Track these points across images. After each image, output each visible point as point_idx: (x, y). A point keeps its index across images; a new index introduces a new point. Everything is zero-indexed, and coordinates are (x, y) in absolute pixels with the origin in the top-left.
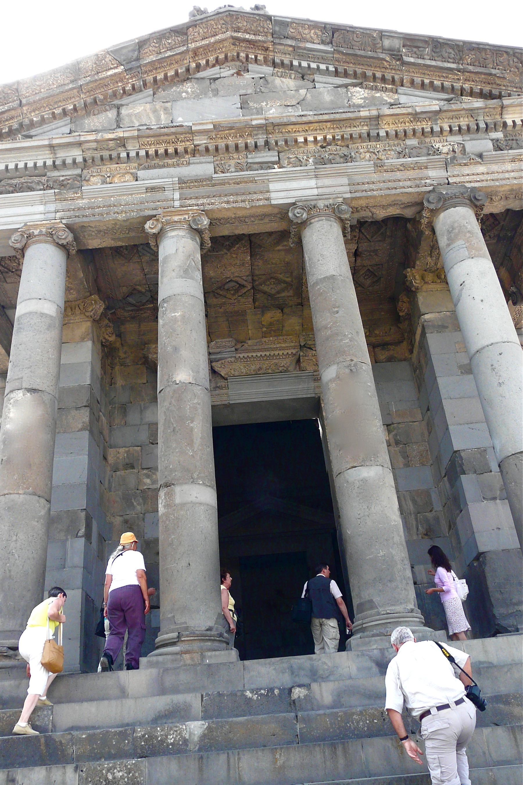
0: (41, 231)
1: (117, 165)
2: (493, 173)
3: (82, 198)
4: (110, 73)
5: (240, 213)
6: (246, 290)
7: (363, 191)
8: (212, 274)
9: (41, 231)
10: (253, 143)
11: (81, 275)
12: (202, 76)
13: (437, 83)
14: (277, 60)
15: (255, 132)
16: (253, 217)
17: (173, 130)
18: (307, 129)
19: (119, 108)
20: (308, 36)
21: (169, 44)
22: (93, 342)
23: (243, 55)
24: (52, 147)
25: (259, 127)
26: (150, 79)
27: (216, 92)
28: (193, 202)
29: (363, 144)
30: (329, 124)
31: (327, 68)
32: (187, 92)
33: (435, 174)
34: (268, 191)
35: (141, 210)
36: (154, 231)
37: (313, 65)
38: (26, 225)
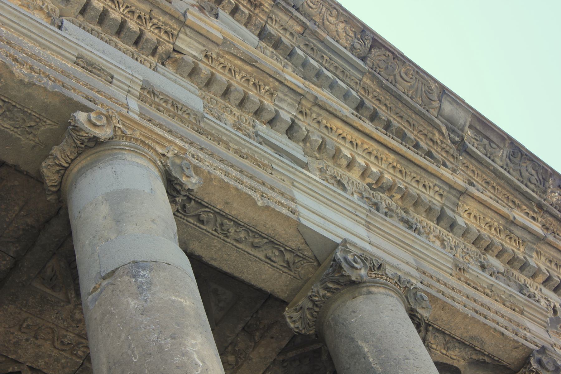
5: (237, 210)
16: (248, 230)
18: (359, 143)
20: (332, 27)
30: (392, 157)
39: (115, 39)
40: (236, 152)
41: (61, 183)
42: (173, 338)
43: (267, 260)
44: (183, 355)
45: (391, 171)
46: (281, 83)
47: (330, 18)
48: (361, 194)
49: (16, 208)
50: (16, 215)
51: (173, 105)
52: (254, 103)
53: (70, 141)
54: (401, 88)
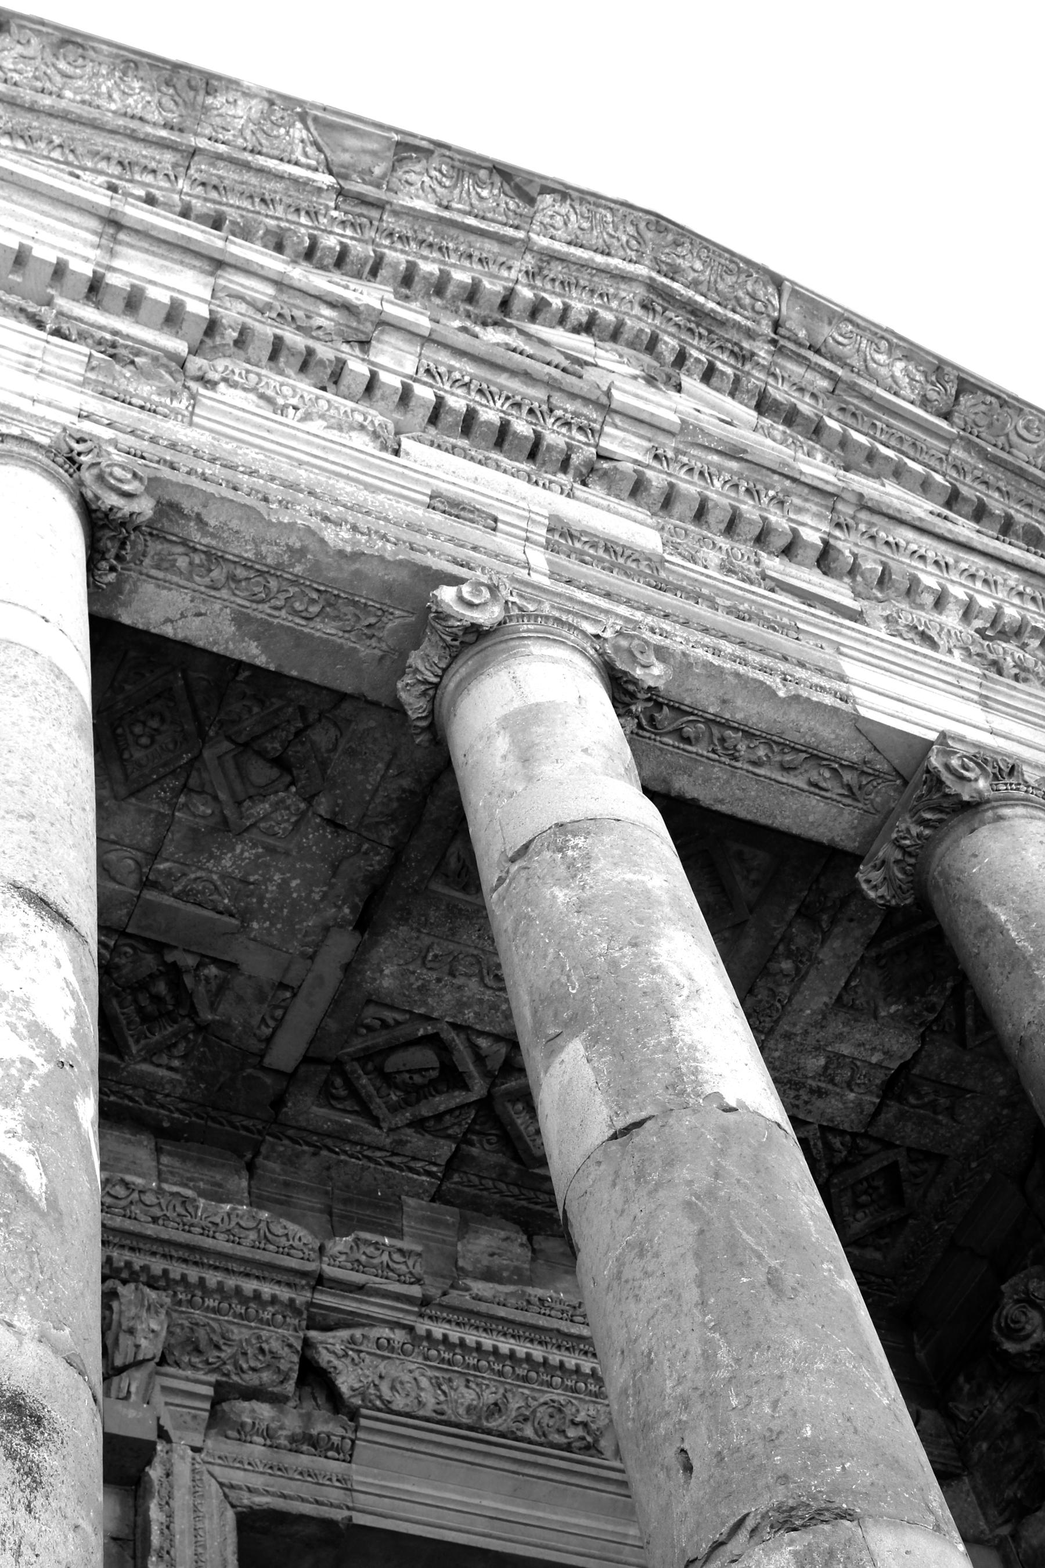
6: (459, 1097)
8: (387, 976)
15: (797, 501)
16: (769, 743)
20: (883, 371)
21: (481, 198)
23: (669, 344)
24: (113, 224)
26: (397, 257)
37: (883, 450)
39: (494, 455)
40: (729, 611)
41: (432, 712)
42: (635, 945)
43: (812, 789)
44: (654, 971)
45: (1016, 601)
46: (794, 480)
47: (877, 356)
48: (967, 649)
49: (380, 765)
50: (383, 777)
51: (606, 550)
52: (751, 522)
53: (435, 638)
54: (1020, 457)
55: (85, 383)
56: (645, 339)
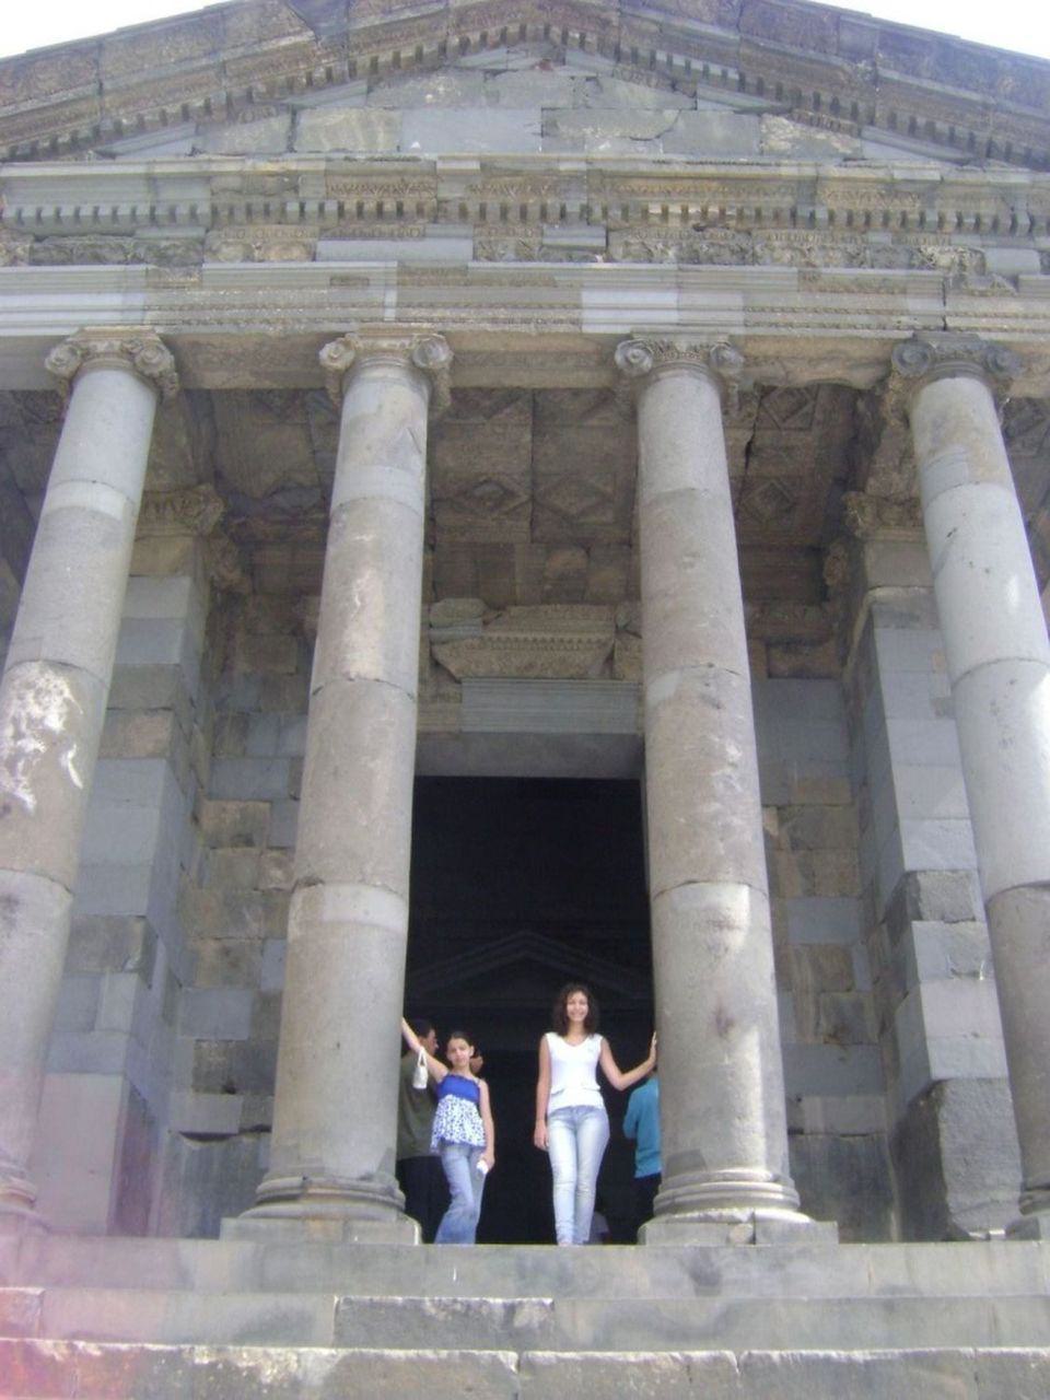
0: (111, 345)
1: (278, 226)
2: (1036, 317)
3: (200, 285)
4: (285, 42)
5: (517, 345)
7: (771, 325)
8: (450, 462)
9: (111, 345)
10: (558, 206)
11: (183, 440)
12: (469, 64)
13: (941, 126)
14: (625, 48)
17: (398, 166)
18: (670, 189)
19: (294, 113)
22: (195, 580)
23: (556, 31)
24: (151, 180)
25: (574, 177)
26: (363, 60)
27: (494, 99)
28: (424, 313)
29: (778, 232)
30: (715, 184)
31: (725, 74)
32: (435, 92)
33: (920, 308)
34: (578, 307)
35: (315, 321)
36: (339, 365)
37: (697, 65)
38: (82, 331)
55: (148, 286)
56: (542, 33)
